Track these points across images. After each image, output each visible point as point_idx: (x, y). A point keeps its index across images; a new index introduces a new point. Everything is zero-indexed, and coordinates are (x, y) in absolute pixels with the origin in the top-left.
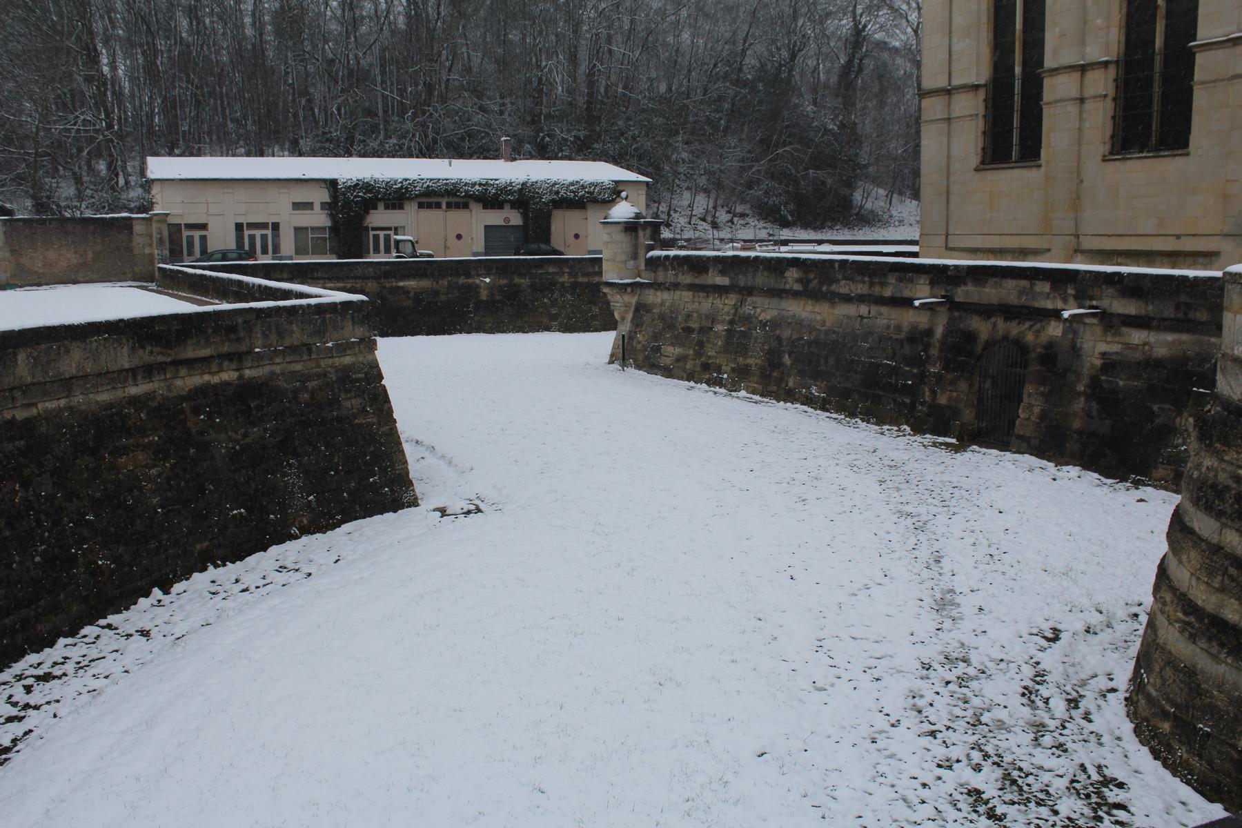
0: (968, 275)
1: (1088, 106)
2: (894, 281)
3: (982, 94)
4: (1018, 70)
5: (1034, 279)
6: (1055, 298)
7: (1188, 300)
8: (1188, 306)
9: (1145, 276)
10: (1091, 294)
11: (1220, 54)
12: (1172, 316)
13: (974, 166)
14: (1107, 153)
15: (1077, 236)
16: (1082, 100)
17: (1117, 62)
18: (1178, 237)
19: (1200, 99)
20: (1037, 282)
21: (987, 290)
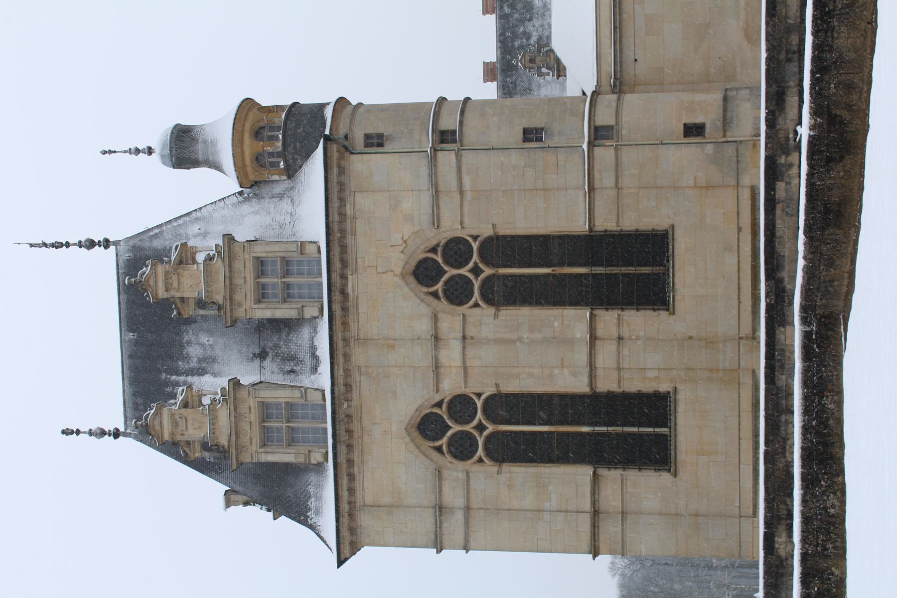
0: (774, 278)
1: (625, 333)
2: (784, 377)
3: (603, 472)
4: (585, 429)
5: (774, 200)
6: (789, 176)
7: (784, 52)
8: (788, 52)
9: (767, 93)
10: (784, 139)
11: (599, 204)
12: (797, 64)
13: (671, 477)
14: (668, 313)
15: (740, 338)
16: (620, 338)
17: (592, 309)
18: (739, 230)
19: (630, 223)
20: (777, 197)
21: (787, 255)
